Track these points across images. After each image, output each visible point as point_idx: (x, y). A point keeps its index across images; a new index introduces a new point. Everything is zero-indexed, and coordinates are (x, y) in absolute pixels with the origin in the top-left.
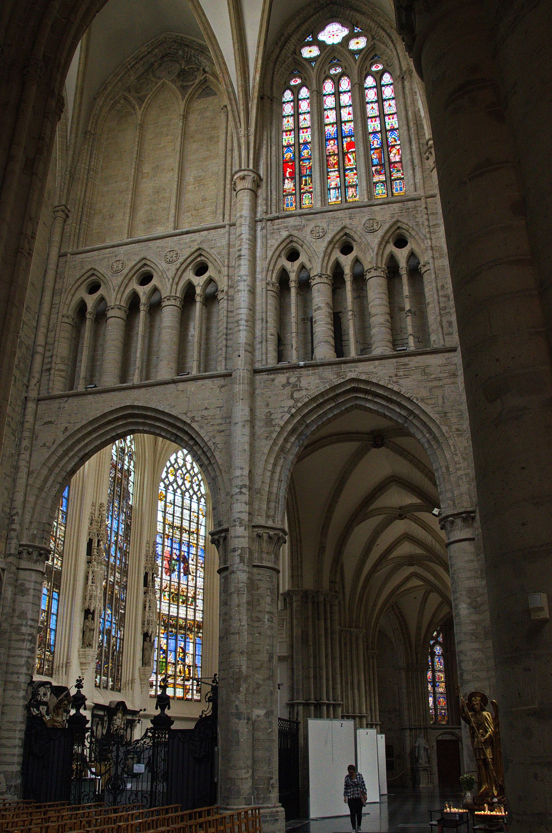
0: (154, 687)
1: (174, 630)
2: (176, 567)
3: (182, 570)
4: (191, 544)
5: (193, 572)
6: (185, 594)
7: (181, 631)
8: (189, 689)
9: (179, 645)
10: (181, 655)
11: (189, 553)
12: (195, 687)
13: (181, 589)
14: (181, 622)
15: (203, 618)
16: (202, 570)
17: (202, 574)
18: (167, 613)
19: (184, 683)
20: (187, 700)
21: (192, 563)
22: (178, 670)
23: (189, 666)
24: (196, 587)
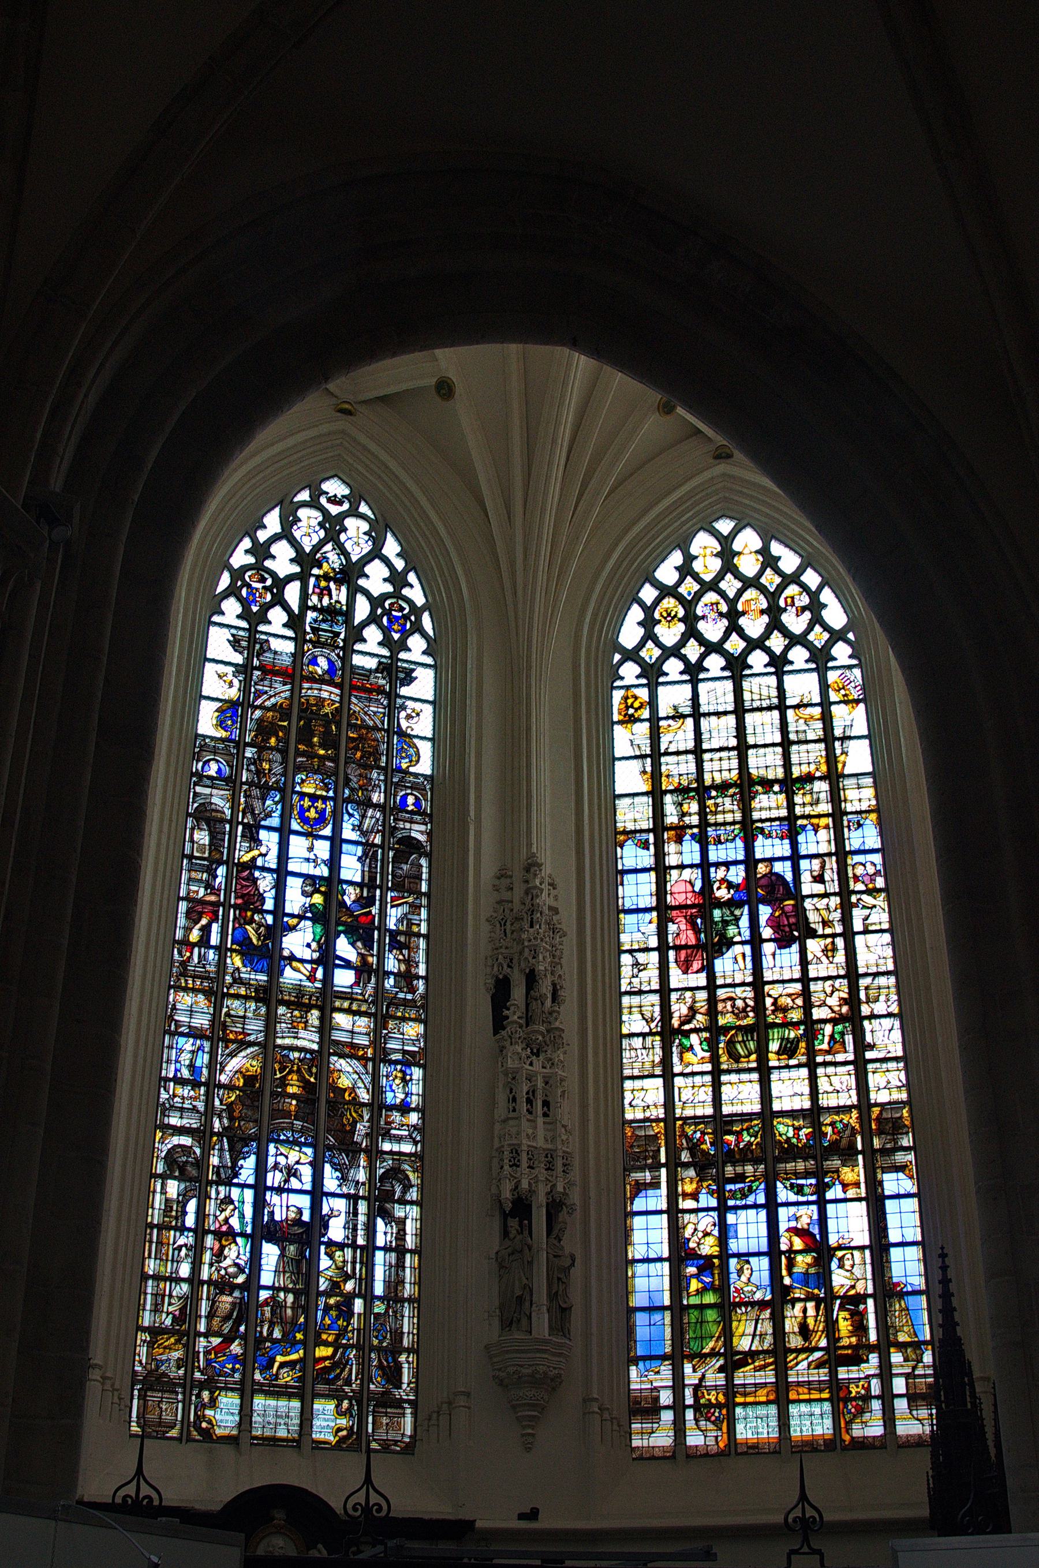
0: (667, 1416)
1: (749, 1169)
2: (731, 931)
3: (767, 933)
4: (800, 822)
5: (825, 923)
6: (795, 1016)
7: (790, 1166)
8: (867, 1398)
9: (783, 1226)
10: (803, 1261)
11: (795, 858)
12: (899, 1385)
13: (769, 1001)
14: (784, 1129)
15: (908, 1086)
16: (881, 901)
17: (881, 918)
18: (709, 1111)
19: (833, 1374)
20: (863, 1444)
21: (819, 888)
22: (791, 1325)
23: (853, 1301)
24: (852, 974)
